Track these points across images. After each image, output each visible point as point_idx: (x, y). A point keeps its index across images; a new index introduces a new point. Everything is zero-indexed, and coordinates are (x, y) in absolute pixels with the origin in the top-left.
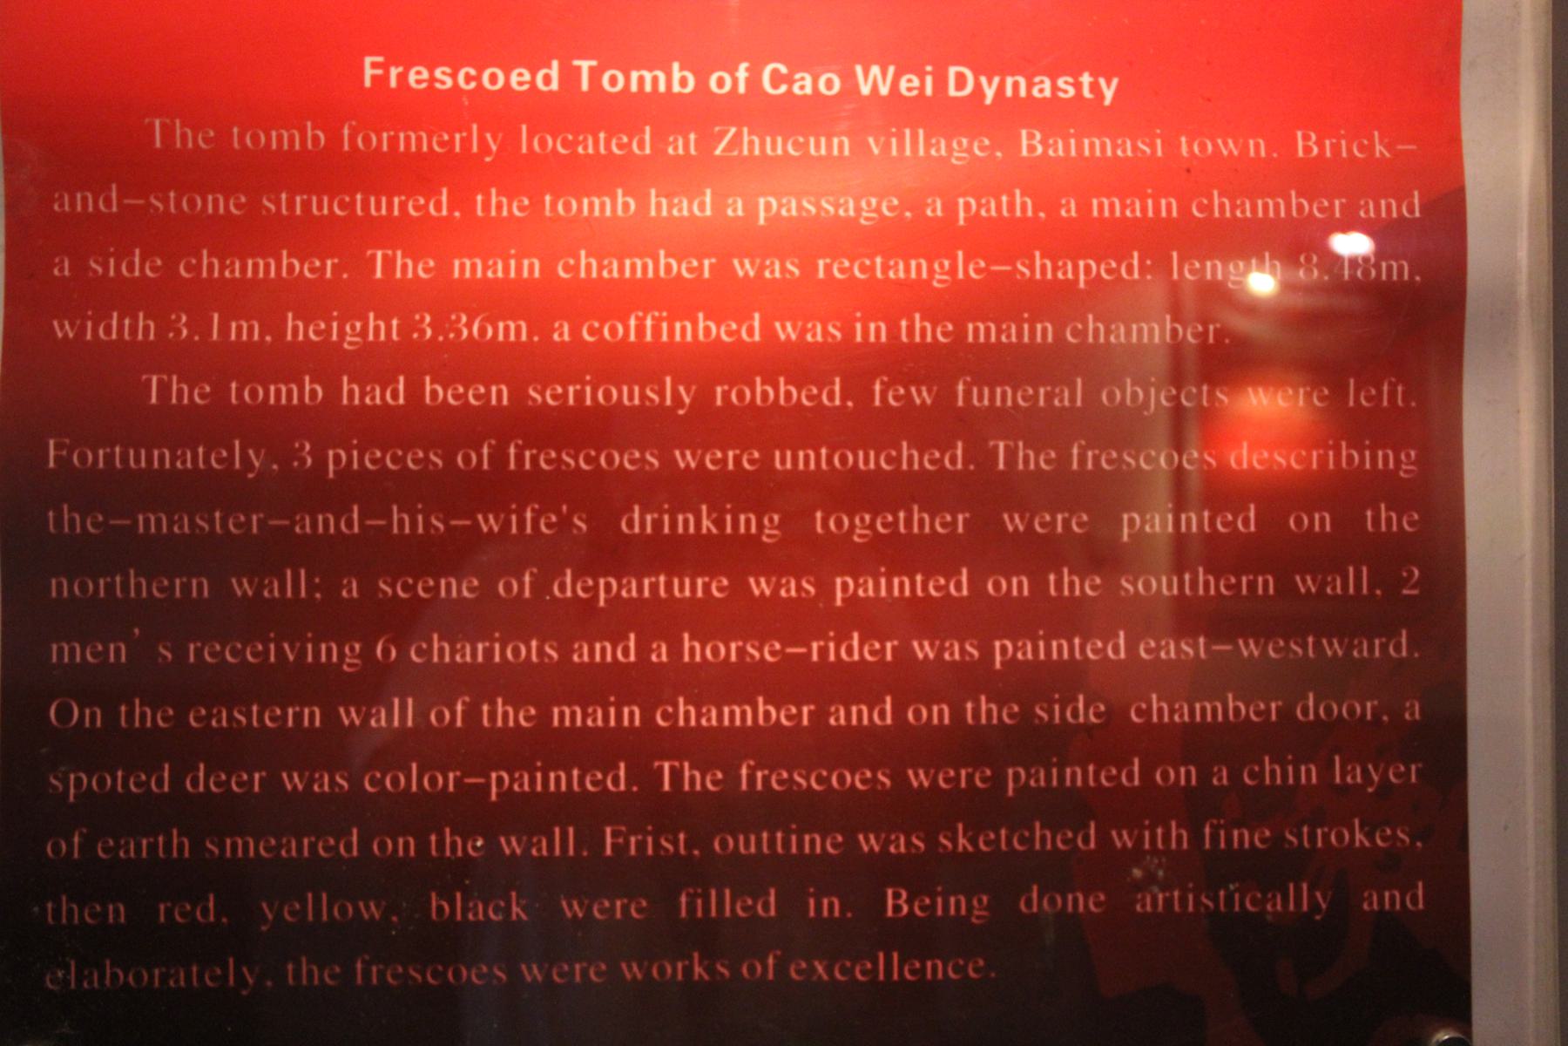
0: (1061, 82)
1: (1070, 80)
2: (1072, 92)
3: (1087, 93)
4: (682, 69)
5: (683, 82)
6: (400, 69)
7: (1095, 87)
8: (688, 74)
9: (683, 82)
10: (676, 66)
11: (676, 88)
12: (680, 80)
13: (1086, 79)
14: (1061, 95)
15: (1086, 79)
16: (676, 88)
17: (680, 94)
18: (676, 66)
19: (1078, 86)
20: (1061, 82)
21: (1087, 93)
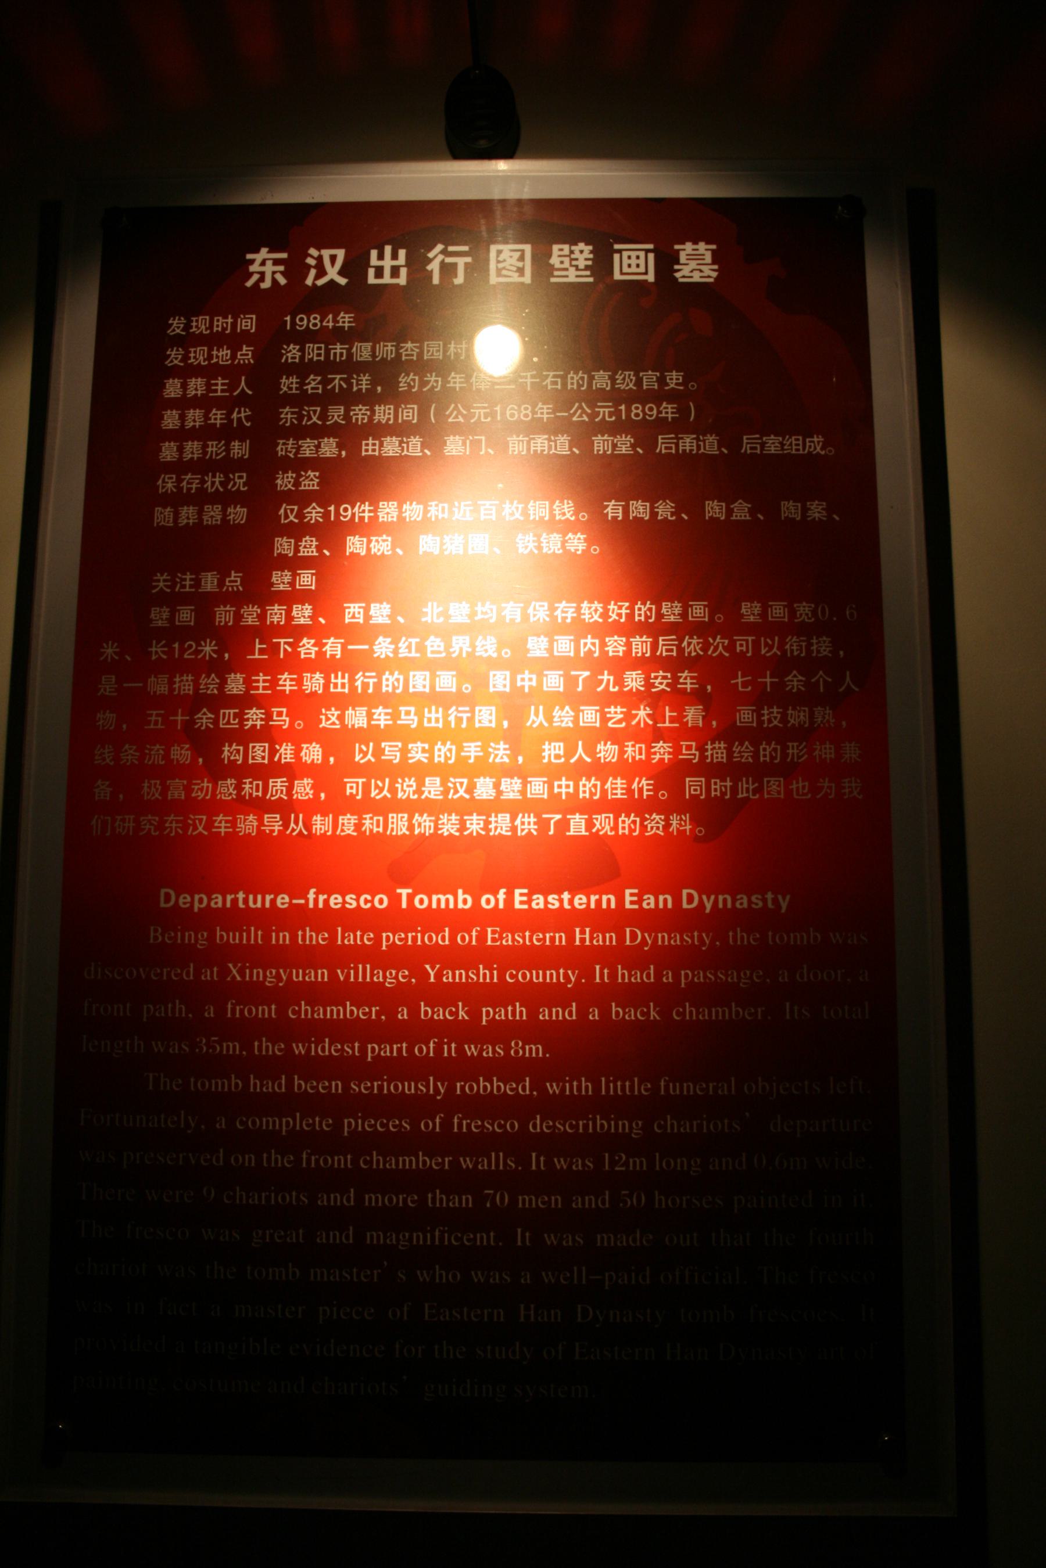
0: (753, 899)
1: (760, 897)
2: (761, 904)
3: (770, 905)
4: (464, 893)
5: (465, 901)
6: (272, 896)
7: (775, 901)
8: (466, 896)
9: (465, 901)
10: (460, 891)
11: (460, 906)
12: (463, 901)
13: (769, 896)
14: (754, 906)
15: (769, 896)
16: (460, 906)
17: (463, 910)
18: (460, 891)
19: (764, 900)
20: (753, 899)
21: (770, 905)
